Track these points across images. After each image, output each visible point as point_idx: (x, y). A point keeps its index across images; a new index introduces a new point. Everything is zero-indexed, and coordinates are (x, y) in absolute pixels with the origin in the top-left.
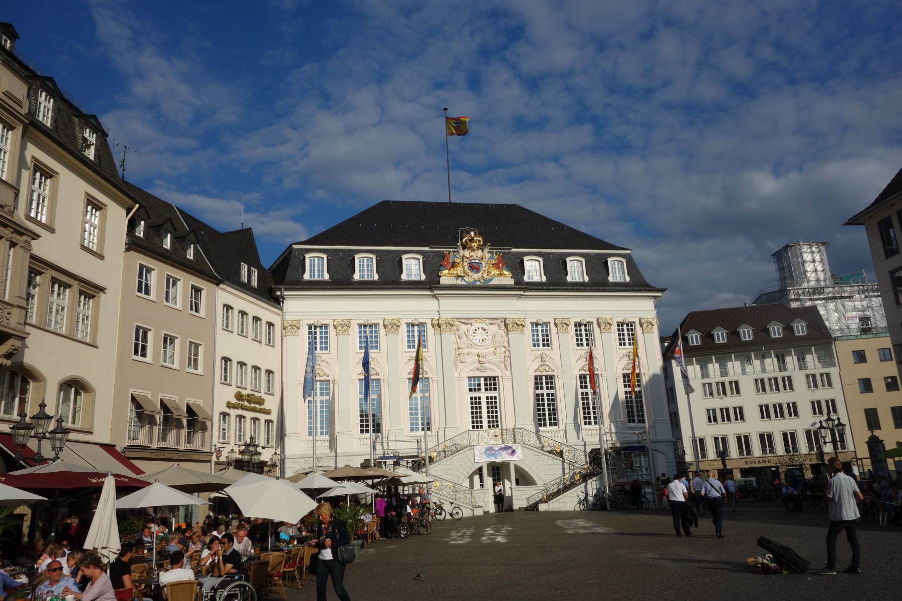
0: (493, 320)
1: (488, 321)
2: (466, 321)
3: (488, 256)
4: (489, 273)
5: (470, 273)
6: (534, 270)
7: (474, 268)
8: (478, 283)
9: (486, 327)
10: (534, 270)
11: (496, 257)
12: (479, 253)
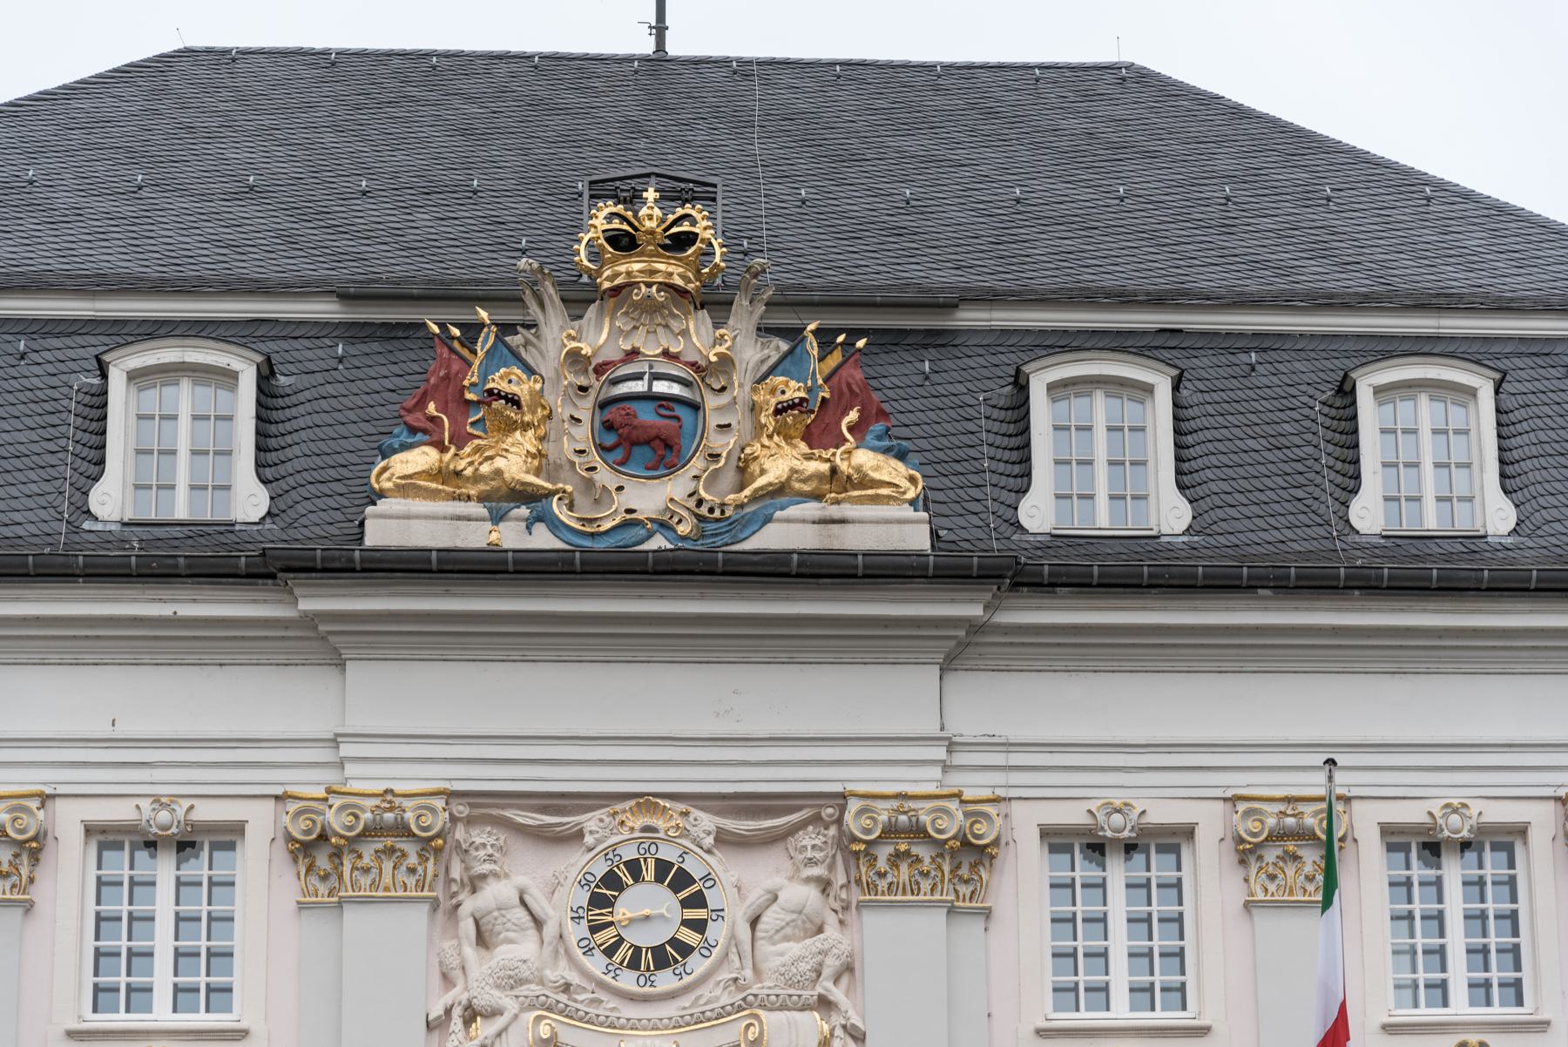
0: (758, 819)
1: (706, 822)
2: (551, 817)
3: (752, 353)
4: (744, 472)
5: (605, 477)
6: (1104, 459)
7: (643, 434)
8: (658, 542)
9: (694, 868)
10: (1104, 459)
11: (819, 369)
12: (698, 336)
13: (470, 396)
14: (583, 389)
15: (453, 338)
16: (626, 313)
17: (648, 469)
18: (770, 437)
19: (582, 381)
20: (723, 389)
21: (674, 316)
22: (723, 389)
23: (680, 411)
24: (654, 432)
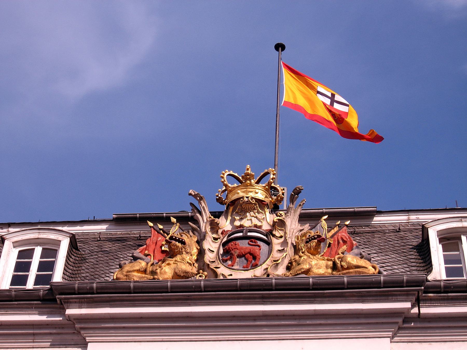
13: (163, 248)
14: (215, 239)
15: (160, 229)
16: (237, 213)
17: (244, 267)
18: (302, 253)
19: (215, 236)
20: (281, 237)
21: (259, 213)
22: (281, 237)
23: (259, 243)
24: (247, 251)
